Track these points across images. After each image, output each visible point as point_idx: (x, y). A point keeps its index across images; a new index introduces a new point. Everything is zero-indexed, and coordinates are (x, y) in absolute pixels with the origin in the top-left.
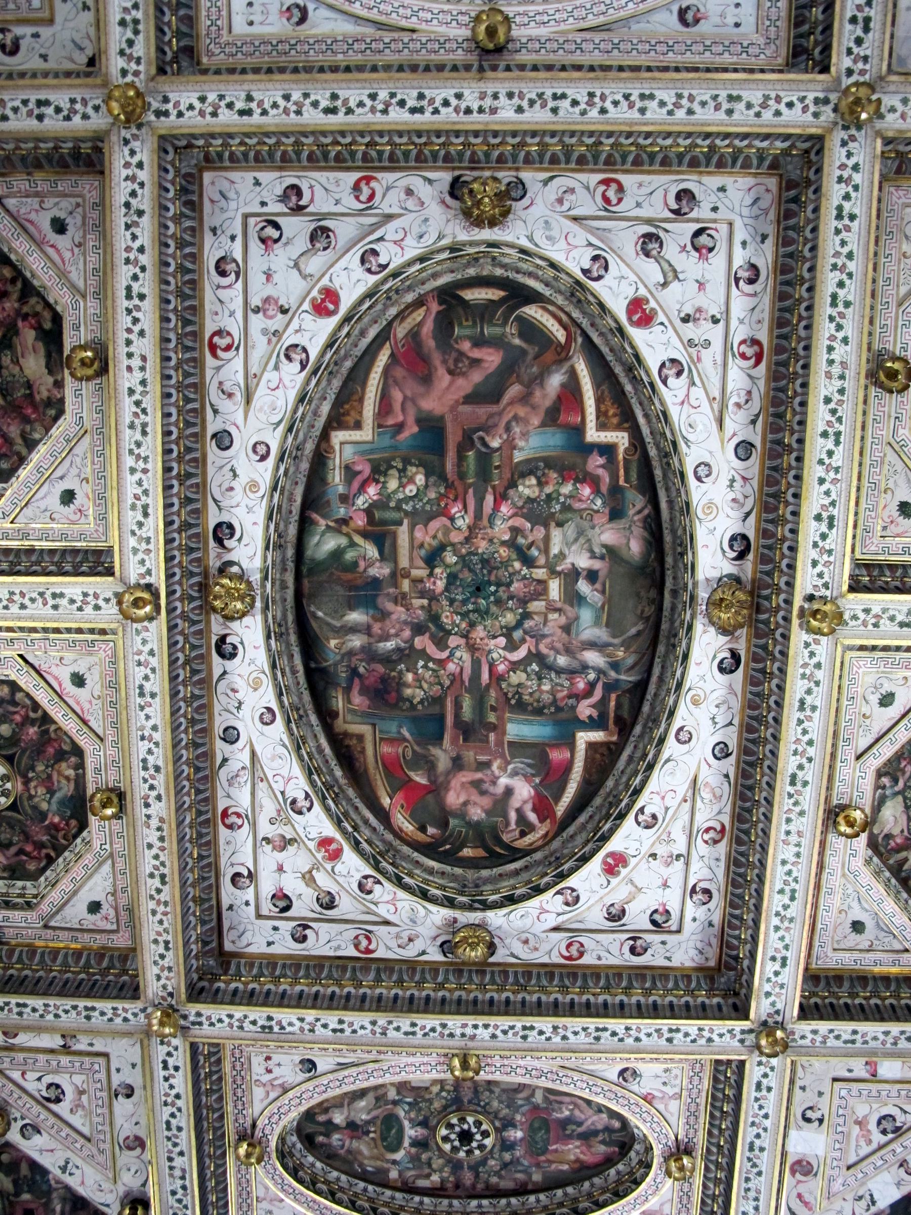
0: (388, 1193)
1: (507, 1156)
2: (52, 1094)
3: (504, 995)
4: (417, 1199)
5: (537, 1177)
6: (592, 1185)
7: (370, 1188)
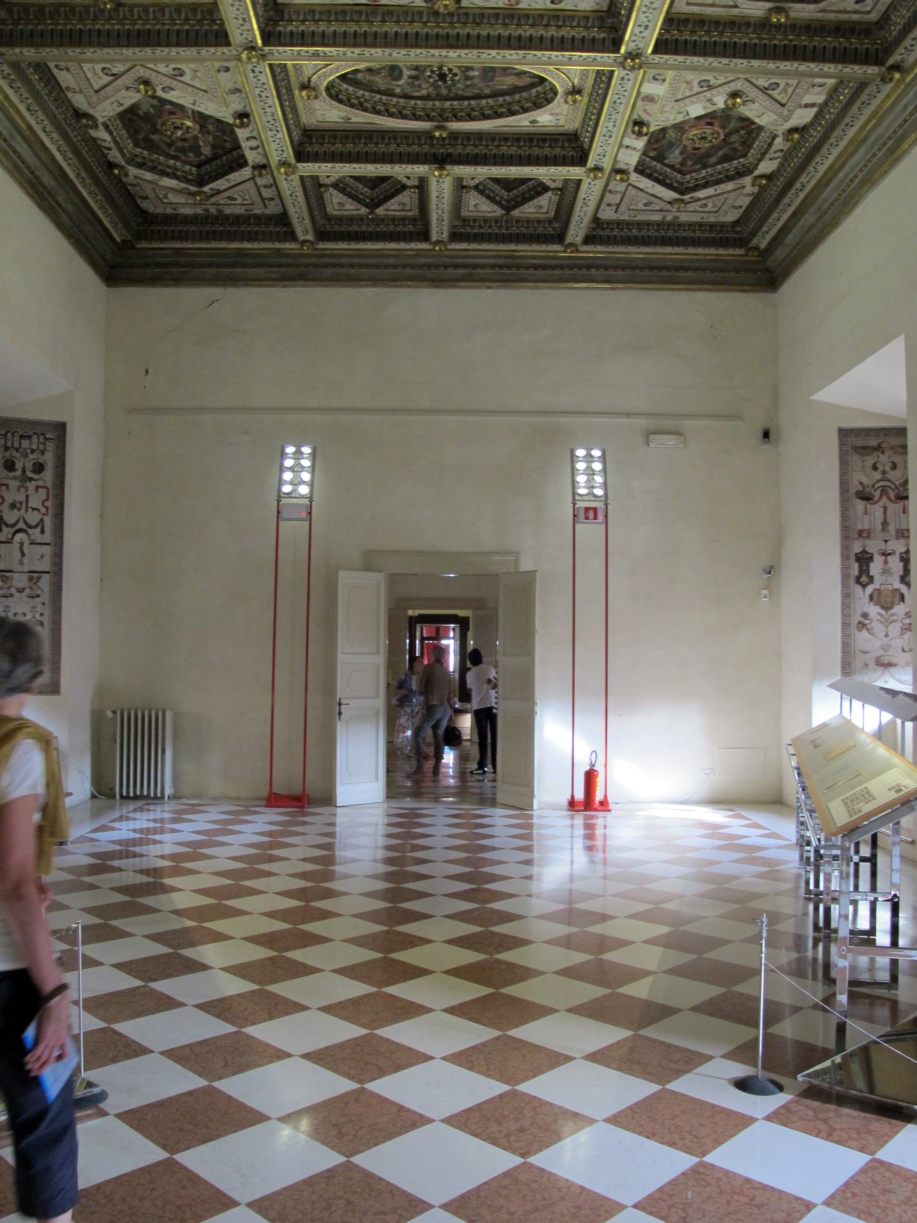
0: (395, 100)
1: (469, 83)
2: (177, 72)
3: (466, 31)
4: (413, 102)
5: (487, 91)
6: (521, 97)
7: (384, 98)
